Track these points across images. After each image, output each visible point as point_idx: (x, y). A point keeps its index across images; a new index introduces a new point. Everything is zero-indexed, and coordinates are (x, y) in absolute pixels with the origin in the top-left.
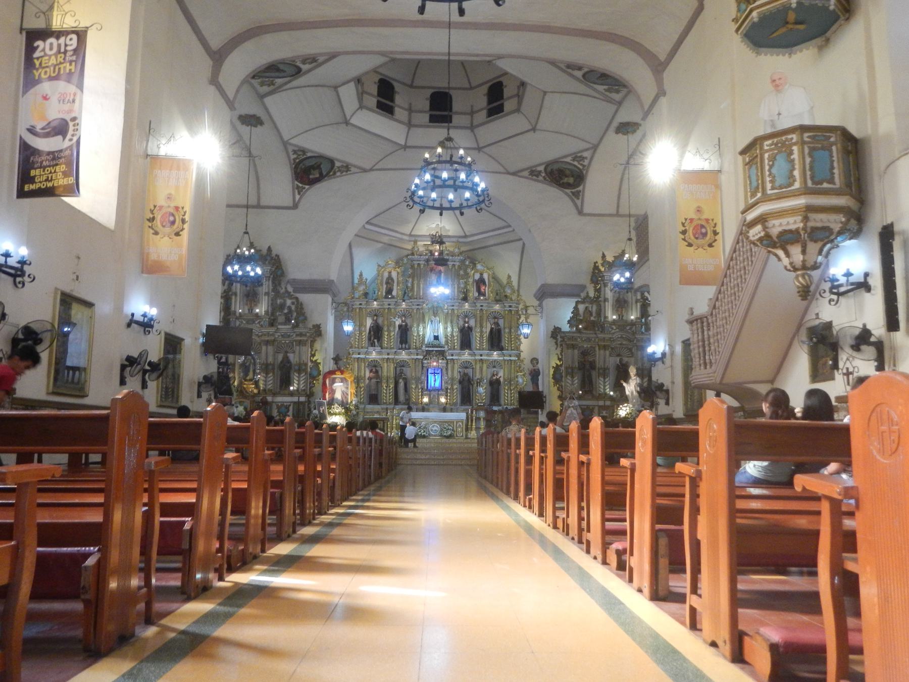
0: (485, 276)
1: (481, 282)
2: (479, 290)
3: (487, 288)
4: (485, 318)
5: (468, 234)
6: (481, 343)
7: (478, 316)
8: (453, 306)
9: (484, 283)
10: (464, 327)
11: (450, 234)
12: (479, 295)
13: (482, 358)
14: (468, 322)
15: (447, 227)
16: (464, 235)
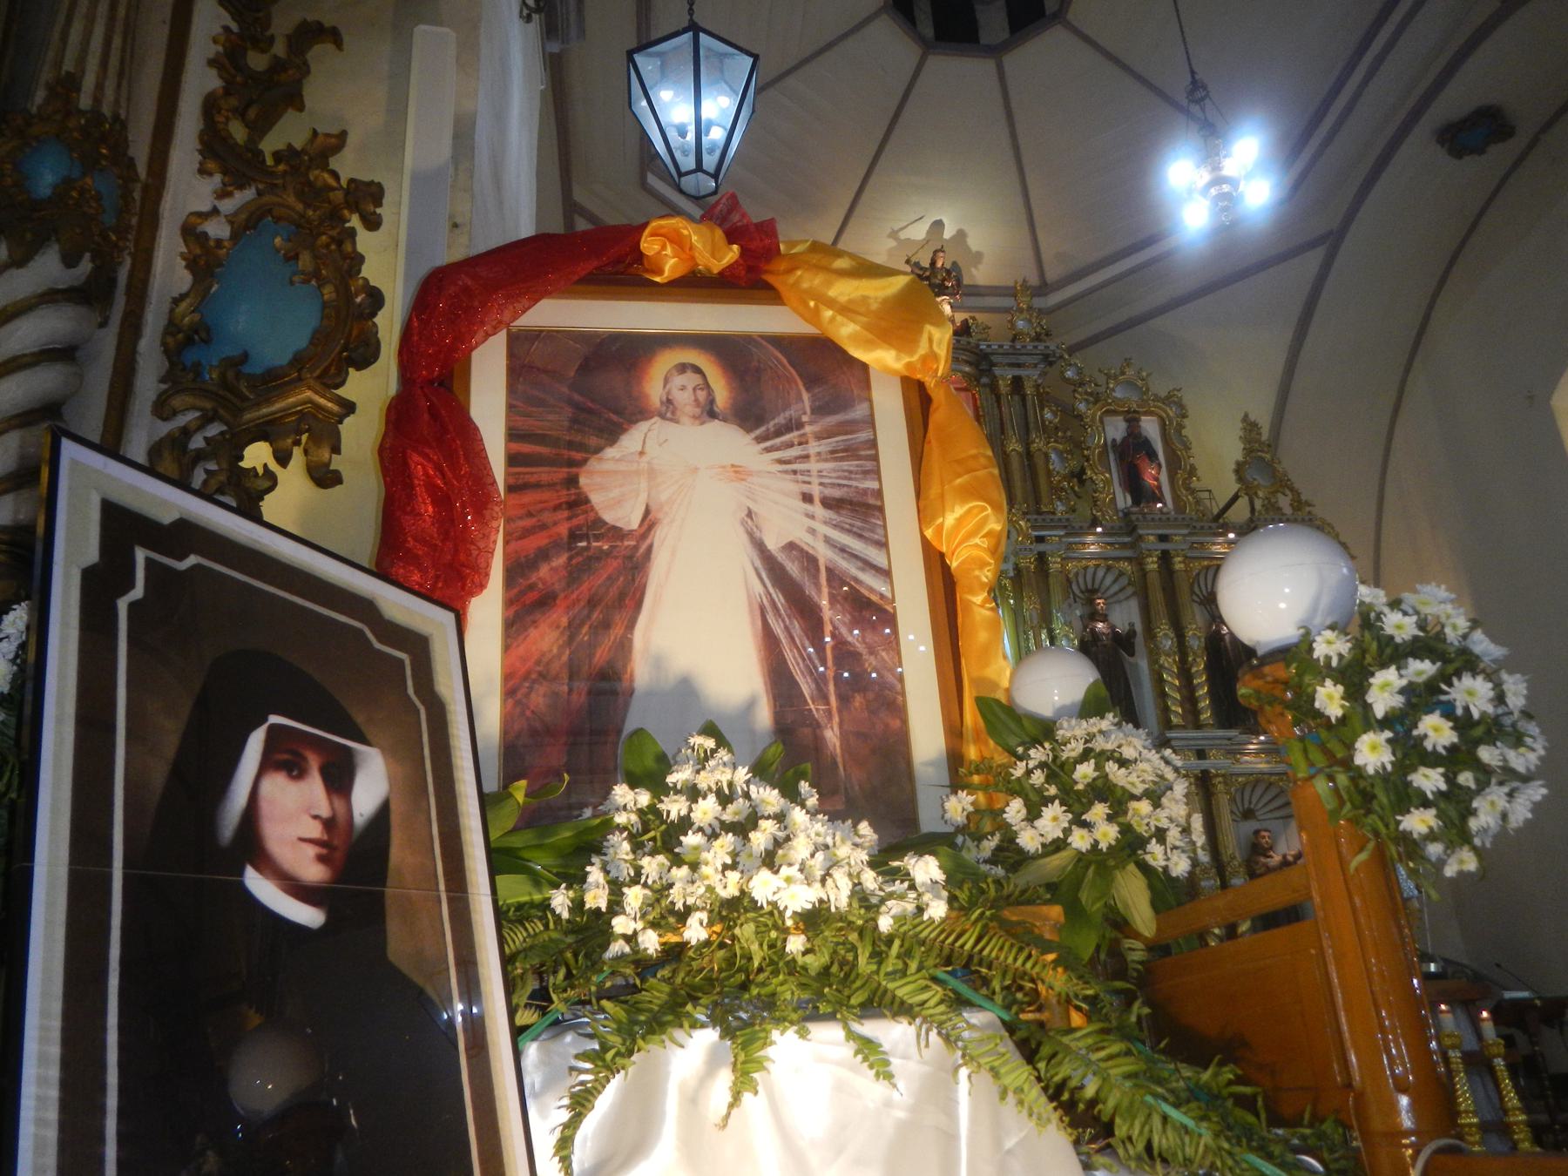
0: (1150, 427)
1: (1133, 451)
2: (1134, 483)
3: (1164, 477)
4: (1184, 597)
5: (1052, 275)
6: (1190, 700)
7: (1154, 581)
8: (1040, 539)
9: (1152, 455)
10: (1095, 635)
11: (979, 275)
12: (1136, 502)
13: (1205, 764)
14: (1104, 619)
15: (974, 243)
16: (1034, 280)
